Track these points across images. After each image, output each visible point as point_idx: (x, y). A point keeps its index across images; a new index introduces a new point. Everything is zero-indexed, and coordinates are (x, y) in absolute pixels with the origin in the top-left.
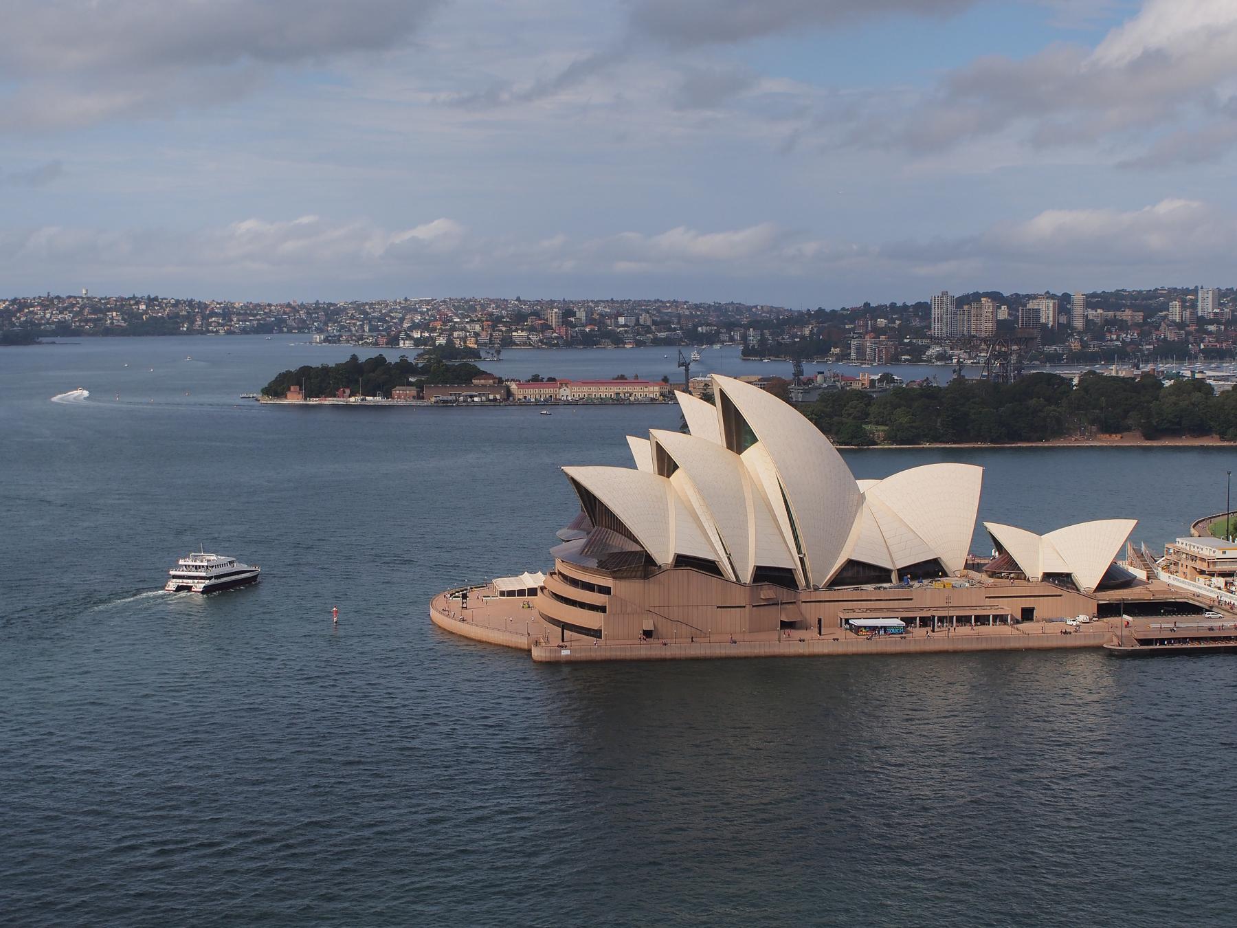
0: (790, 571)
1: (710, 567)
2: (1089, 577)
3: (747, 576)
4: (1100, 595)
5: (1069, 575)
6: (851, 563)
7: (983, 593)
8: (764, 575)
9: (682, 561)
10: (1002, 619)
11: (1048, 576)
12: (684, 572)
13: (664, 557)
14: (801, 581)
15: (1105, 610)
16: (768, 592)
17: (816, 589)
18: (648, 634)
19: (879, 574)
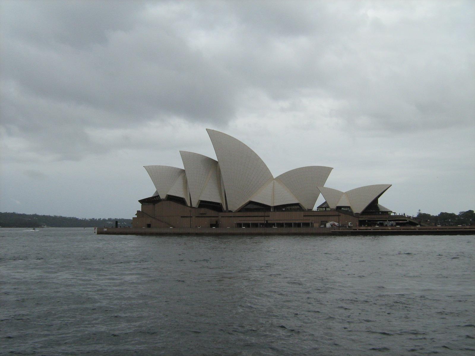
0: (218, 204)
1: (180, 201)
2: (358, 208)
3: (195, 204)
4: (360, 216)
5: (349, 207)
6: (251, 203)
7: (302, 215)
8: (203, 204)
9: (170, 198)
10: (307, 225)
11: (339, 208)
12: (172, 203)
13: (163, 196)
14: (224, 207)
15: (362, 223)
16: (203, 210)
17: (230, 211)
18: (149, 226)
19: (266, 208)
